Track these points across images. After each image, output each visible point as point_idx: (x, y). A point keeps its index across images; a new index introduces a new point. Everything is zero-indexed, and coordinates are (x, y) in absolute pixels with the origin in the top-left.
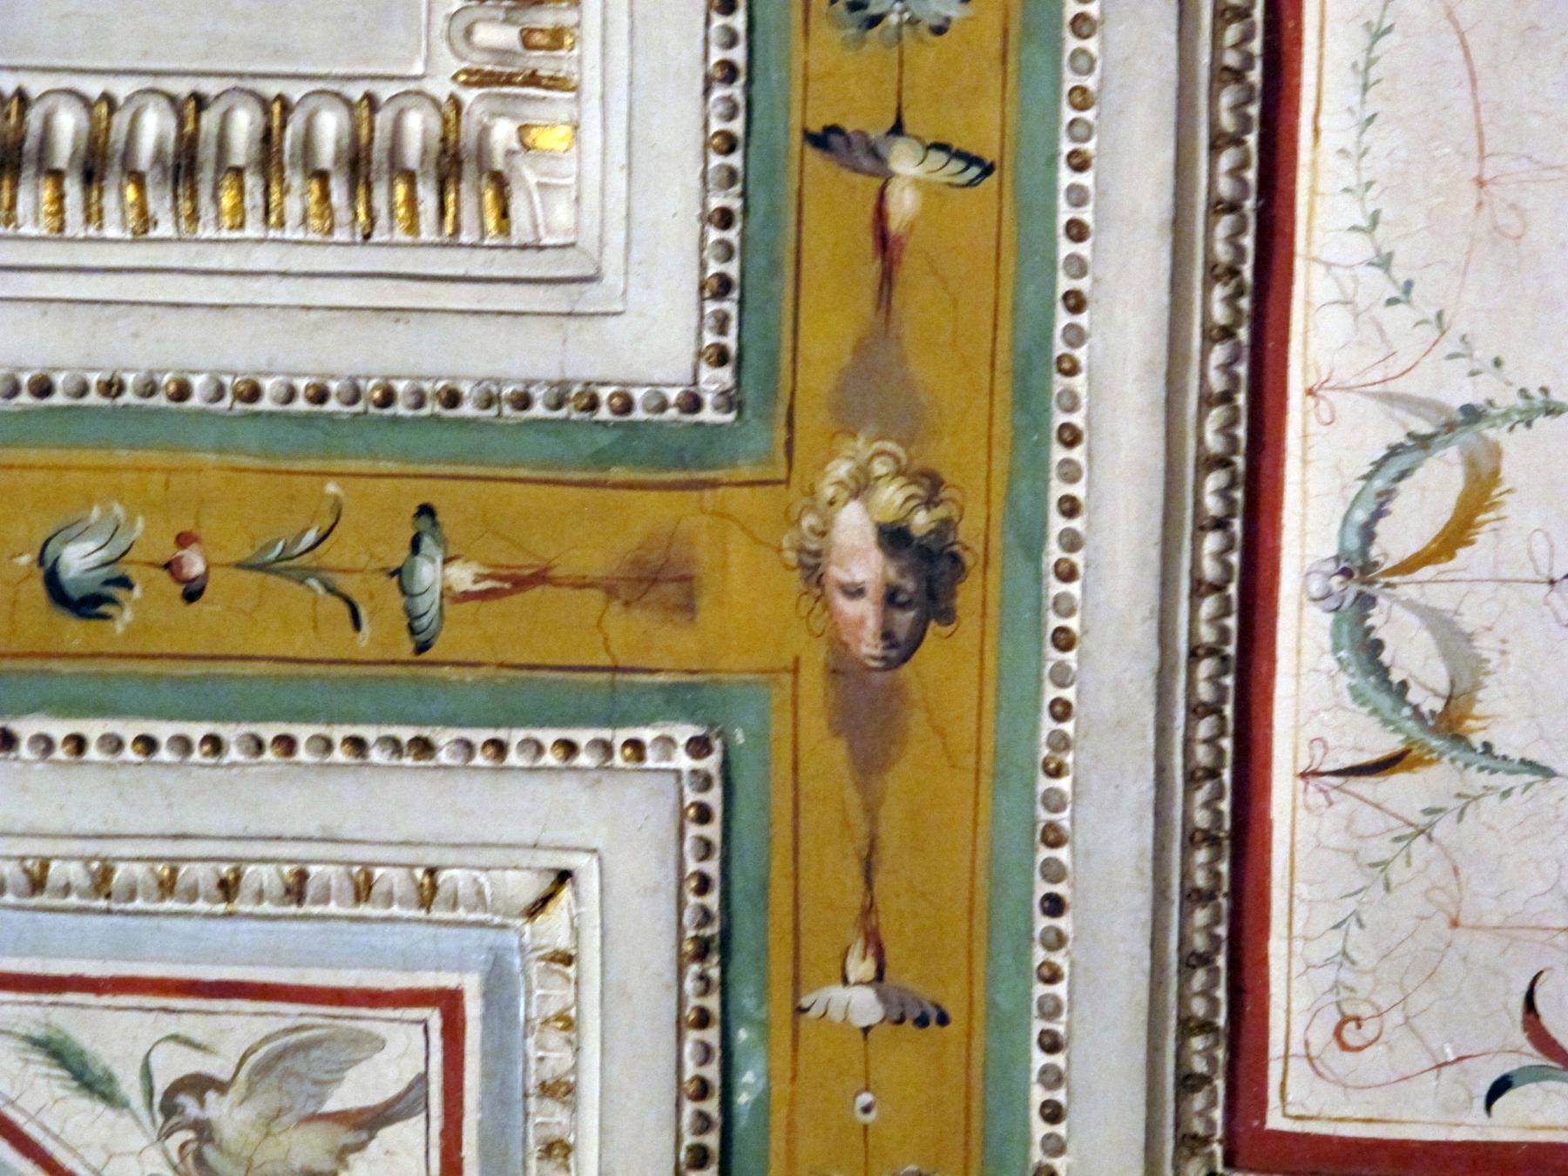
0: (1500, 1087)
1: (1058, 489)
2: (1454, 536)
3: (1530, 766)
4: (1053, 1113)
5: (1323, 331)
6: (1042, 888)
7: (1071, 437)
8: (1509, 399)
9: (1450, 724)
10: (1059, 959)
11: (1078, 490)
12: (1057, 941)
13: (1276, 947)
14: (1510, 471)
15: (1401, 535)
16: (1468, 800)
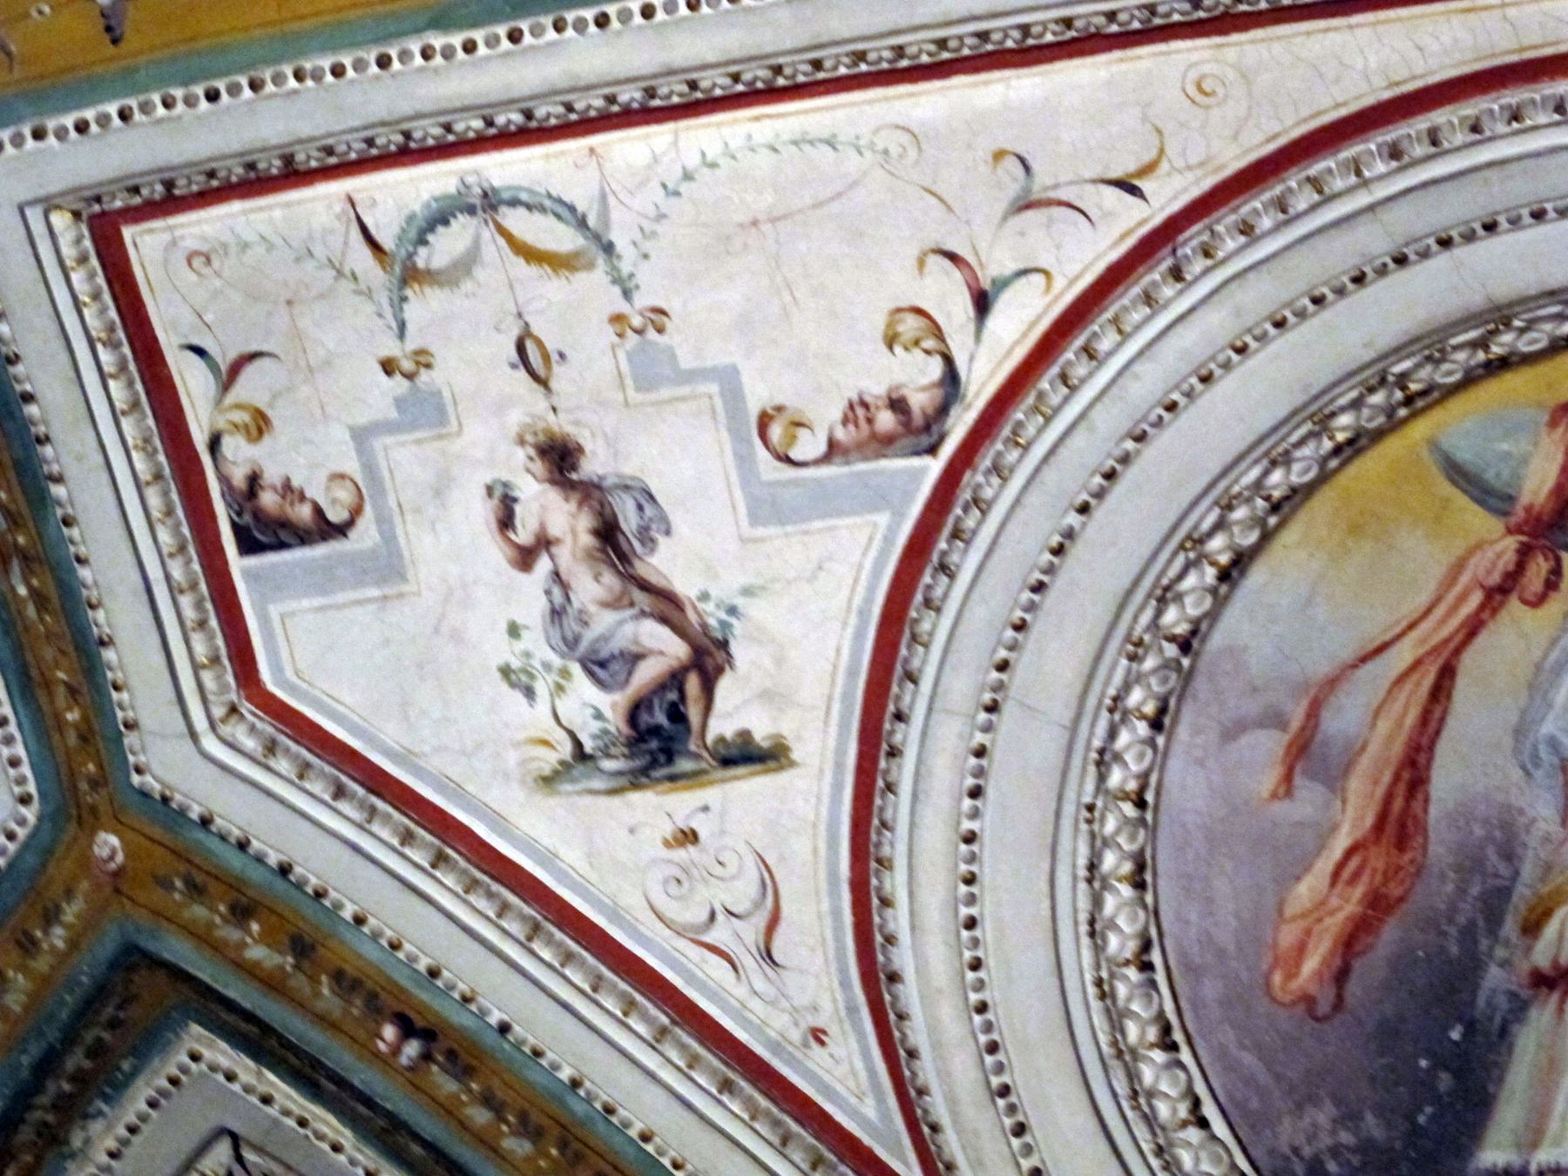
0: (199, 351)
1: (478, 35)
2: (530, 254)
3: (402, 326)
4: (82, 127)
5: (628, 148)
6: (221, 85)
7: (515, 36)
8: (625, 267)
9: (411, 275)
10: (180, 108)
11: (482, 50)
12: (190, 102)
13: (236, 206)
14: (581, 278)
15: (517, 221)
16: (369, 294)
